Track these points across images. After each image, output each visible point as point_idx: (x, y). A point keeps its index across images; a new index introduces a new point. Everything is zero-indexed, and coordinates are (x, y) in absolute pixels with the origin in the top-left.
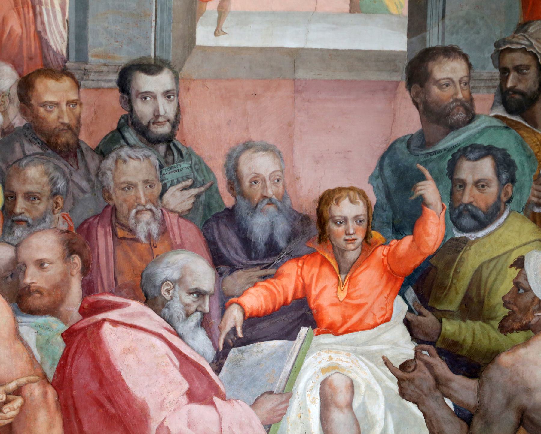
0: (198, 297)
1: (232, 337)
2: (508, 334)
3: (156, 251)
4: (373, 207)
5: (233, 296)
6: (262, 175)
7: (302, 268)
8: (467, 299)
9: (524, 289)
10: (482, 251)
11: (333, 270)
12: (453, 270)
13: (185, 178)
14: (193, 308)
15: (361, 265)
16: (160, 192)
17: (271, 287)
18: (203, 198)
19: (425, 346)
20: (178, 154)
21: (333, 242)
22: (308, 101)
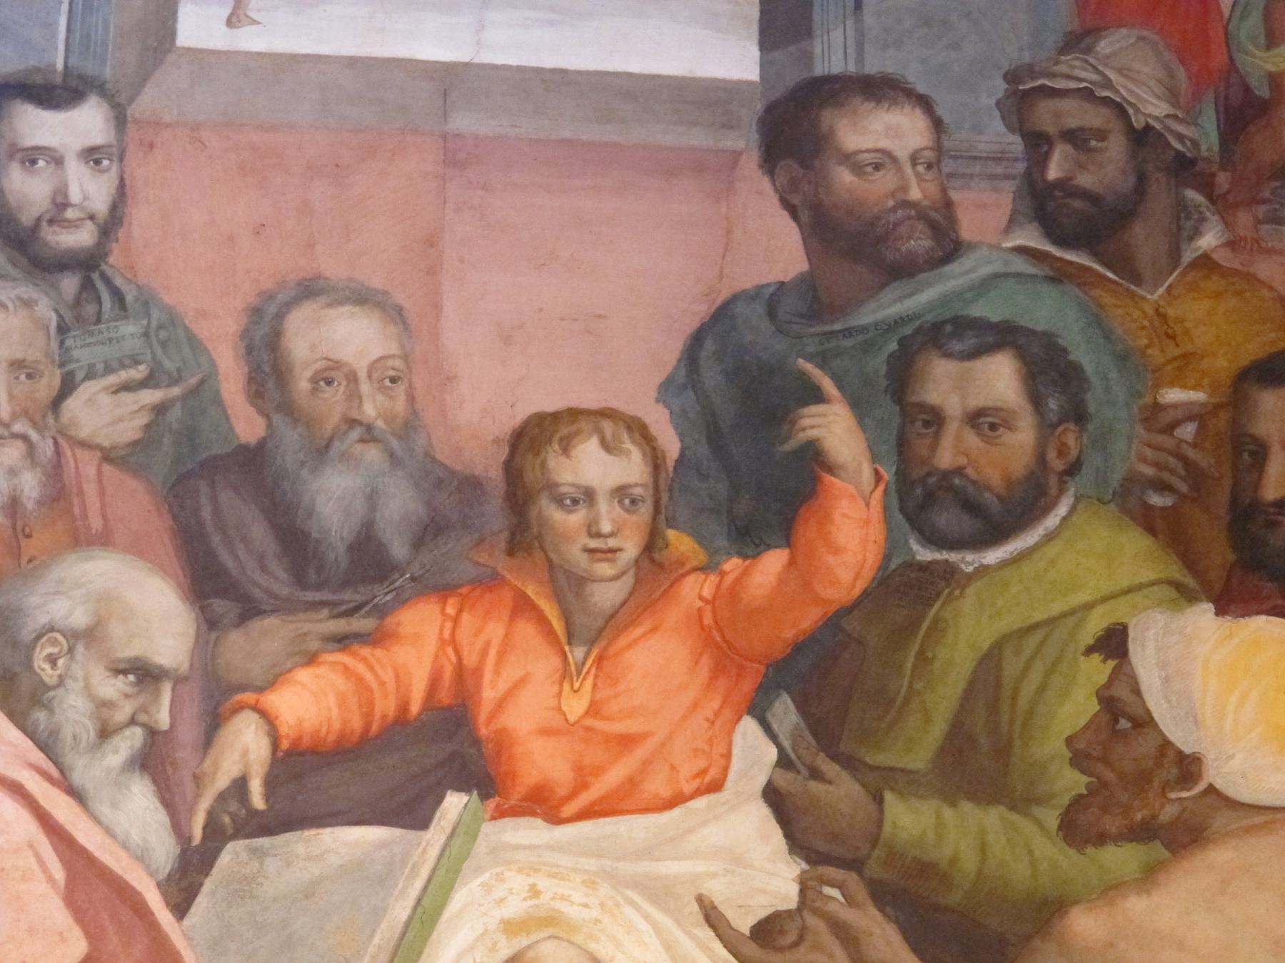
0: (139, 682)
1: (234, 806)
2: (1090, 850)
3: (30, 548)
4: (670, 464)
5: (242, 688)
6: (347, 364)
7: (456, 621)
9: (1130, 718)
10: (1000, 603)
11: (549, 633)
12: (913, 653)
13: (127, 362)
14: (122, 715)
15: (632, 623)
16: (54, 393)
17: (361, 668)
18: (175, 414)
20: (113, 302)
21: (552, 556)
22: (484, 188)
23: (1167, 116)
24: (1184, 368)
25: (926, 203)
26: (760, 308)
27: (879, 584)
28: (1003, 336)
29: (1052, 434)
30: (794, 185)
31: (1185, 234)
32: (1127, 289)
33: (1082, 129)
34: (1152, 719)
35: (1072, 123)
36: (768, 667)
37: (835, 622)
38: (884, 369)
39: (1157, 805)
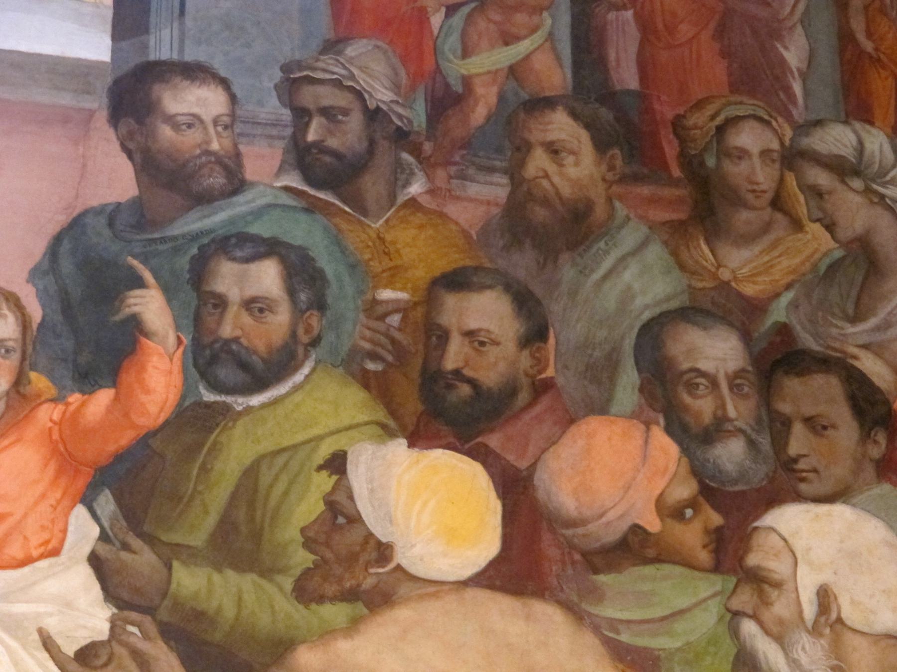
2: (314, 606)
4: (35, 326)
8: (226, 527)
10: (260, 433)
19: (134, 615)
23: (392, 101)
24: (393, 276)
25: (222, 153)
26: (103, 221)
27: (177, 416)
28: (270, 248)
29: (302, 317)
30: (131, 135)
31: (400, 183)
32: (359, 220)
33: (332, 107)
34: (361, 517)
35: (326, 102)
36: (96, 470)
37: (145, 440)
38: (187, 267)
39: (361, 577)
